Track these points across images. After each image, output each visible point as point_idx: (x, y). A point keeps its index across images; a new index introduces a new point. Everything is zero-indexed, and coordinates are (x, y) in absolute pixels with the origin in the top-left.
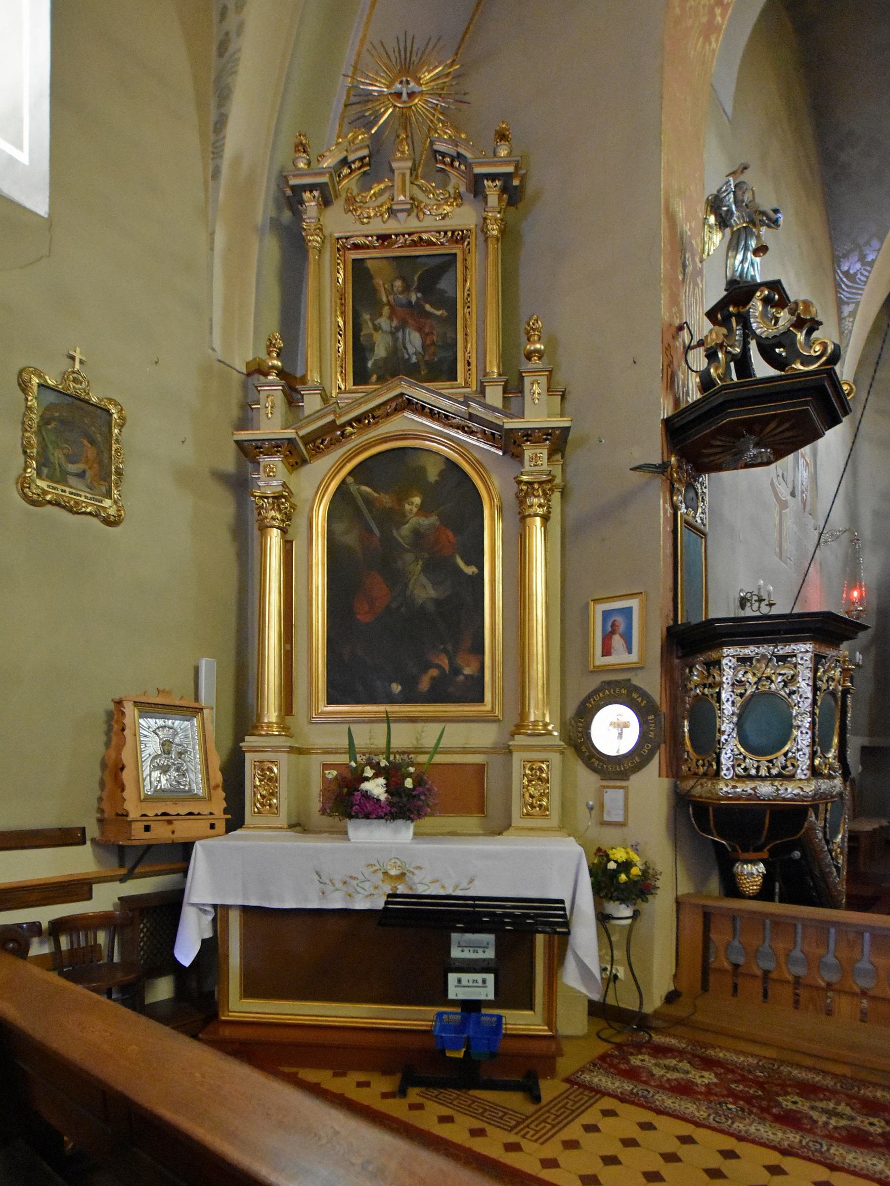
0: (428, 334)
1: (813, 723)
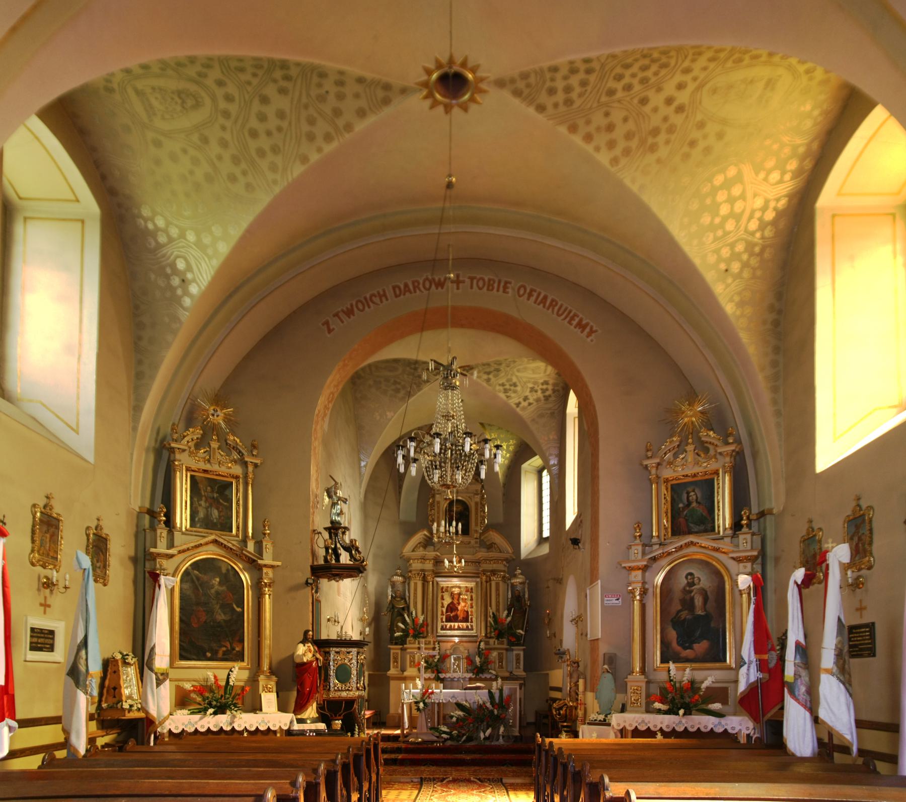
0: (221, 512)
1: (357, 673)
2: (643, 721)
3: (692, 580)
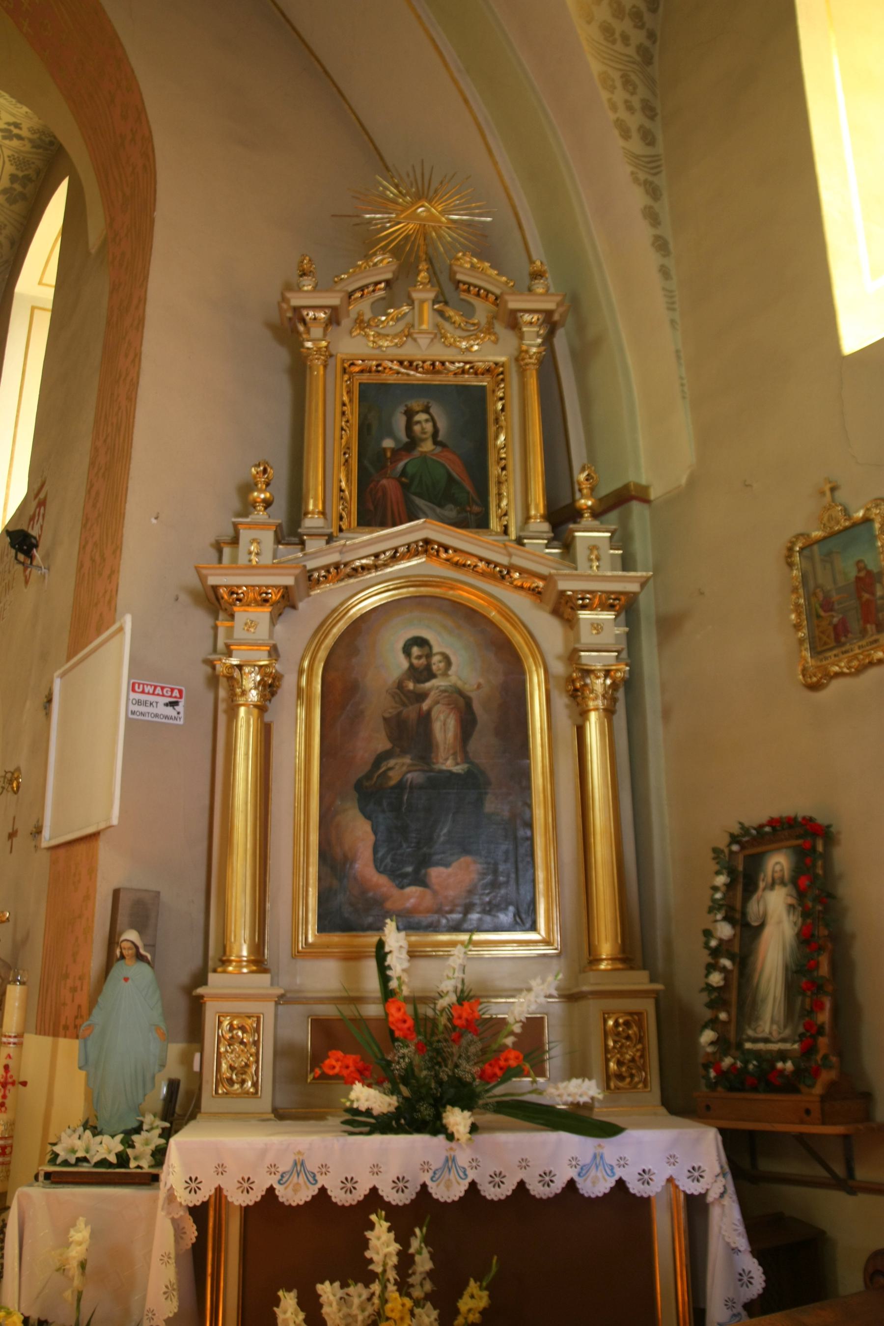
2: (299, 1166)
3: (423, 661)
